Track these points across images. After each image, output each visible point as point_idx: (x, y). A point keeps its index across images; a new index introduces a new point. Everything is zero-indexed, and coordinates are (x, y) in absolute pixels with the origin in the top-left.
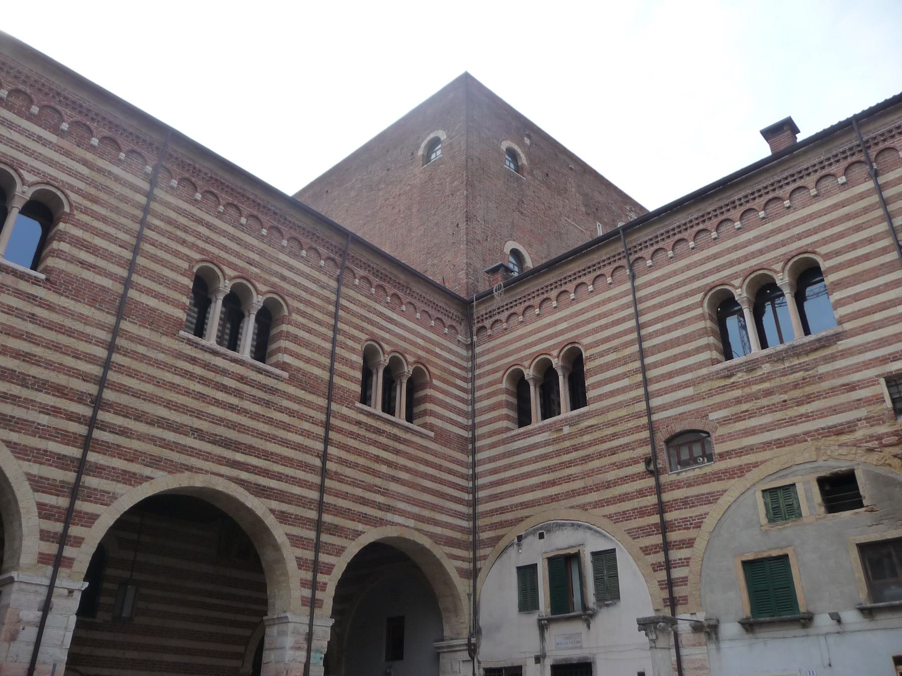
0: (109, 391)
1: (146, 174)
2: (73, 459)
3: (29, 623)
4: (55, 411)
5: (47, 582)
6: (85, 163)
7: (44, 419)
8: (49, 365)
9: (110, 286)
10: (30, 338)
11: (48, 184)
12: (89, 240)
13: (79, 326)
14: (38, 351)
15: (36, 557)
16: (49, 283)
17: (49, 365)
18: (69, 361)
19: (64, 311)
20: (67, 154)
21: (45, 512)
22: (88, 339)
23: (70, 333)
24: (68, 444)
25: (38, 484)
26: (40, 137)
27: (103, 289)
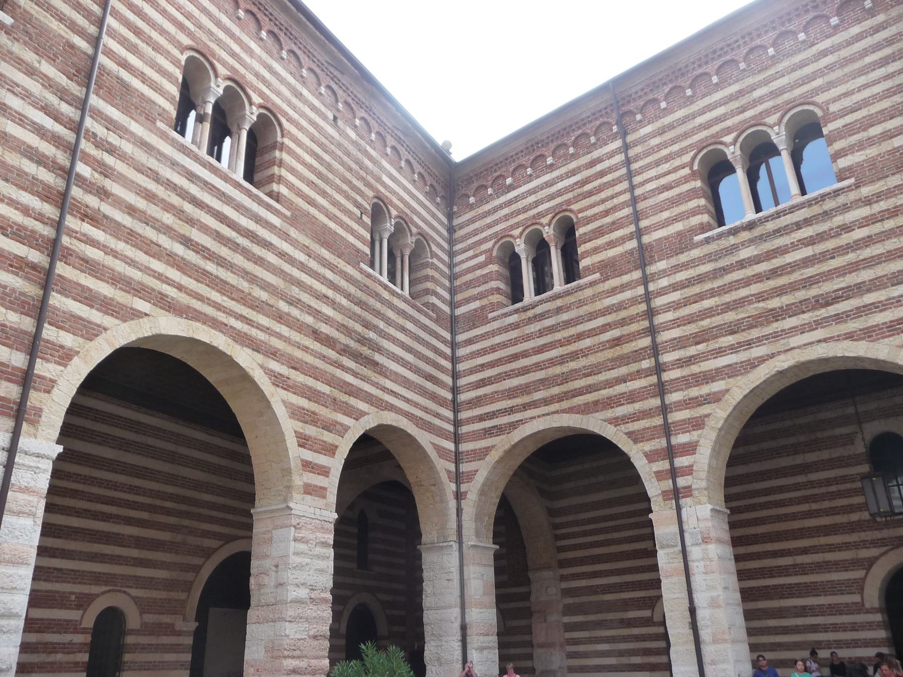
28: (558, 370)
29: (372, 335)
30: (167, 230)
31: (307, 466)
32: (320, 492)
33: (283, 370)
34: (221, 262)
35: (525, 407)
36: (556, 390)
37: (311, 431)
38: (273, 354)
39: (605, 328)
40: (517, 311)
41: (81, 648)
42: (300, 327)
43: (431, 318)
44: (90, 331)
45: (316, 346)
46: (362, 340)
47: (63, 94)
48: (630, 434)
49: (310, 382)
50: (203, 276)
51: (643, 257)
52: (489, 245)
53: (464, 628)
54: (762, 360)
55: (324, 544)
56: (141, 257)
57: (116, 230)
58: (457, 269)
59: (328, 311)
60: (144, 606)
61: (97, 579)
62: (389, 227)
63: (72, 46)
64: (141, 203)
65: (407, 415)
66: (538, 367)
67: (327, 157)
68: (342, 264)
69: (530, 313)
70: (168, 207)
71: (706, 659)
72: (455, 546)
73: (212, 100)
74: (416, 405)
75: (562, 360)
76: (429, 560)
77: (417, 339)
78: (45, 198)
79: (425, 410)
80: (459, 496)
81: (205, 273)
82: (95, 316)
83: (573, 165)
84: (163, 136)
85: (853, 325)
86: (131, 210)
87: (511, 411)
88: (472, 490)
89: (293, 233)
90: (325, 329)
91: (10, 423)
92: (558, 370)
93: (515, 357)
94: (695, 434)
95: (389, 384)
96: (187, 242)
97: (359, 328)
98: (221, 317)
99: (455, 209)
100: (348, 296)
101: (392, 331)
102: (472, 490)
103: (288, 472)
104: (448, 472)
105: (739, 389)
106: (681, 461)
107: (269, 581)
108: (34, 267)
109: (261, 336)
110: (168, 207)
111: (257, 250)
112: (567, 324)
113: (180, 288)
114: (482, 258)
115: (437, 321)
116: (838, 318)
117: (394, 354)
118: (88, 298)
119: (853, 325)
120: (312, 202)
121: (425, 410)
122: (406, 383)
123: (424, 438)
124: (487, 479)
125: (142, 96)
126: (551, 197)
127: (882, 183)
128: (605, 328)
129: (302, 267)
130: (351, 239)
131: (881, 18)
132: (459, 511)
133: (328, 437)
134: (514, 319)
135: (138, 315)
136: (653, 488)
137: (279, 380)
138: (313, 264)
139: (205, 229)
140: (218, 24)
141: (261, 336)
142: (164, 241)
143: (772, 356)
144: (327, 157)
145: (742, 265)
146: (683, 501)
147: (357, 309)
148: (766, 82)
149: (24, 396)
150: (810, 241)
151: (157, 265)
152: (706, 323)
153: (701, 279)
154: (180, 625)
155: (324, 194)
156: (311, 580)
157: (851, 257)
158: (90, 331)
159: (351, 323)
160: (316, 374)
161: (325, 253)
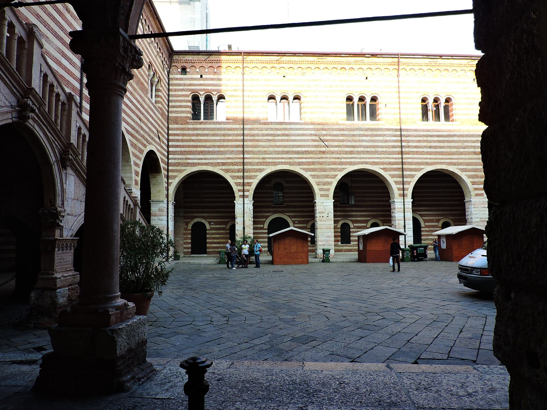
33: (465, 167)
34: (441, 147)
38: (461, 164)
42: (469, 153)
44: (412, 176)
49: (474, 167)
56: (420, 156)
57: (414, 153)
61: (440, 215)
64: (417, 144)
70: (424, 141)
78: (398, 154)
82: (413, 173)
86: (416, 147)
96: (430, 147)
98: (443, 161)
103: (470, 192)
109: (456, 161)
110: (424, 141)
113: (431, 159)
118: (411, 170)
135: (422, 169)
137: (463, 170)
139: (434, 141)
141: (456, 161)
158: (412, 176)
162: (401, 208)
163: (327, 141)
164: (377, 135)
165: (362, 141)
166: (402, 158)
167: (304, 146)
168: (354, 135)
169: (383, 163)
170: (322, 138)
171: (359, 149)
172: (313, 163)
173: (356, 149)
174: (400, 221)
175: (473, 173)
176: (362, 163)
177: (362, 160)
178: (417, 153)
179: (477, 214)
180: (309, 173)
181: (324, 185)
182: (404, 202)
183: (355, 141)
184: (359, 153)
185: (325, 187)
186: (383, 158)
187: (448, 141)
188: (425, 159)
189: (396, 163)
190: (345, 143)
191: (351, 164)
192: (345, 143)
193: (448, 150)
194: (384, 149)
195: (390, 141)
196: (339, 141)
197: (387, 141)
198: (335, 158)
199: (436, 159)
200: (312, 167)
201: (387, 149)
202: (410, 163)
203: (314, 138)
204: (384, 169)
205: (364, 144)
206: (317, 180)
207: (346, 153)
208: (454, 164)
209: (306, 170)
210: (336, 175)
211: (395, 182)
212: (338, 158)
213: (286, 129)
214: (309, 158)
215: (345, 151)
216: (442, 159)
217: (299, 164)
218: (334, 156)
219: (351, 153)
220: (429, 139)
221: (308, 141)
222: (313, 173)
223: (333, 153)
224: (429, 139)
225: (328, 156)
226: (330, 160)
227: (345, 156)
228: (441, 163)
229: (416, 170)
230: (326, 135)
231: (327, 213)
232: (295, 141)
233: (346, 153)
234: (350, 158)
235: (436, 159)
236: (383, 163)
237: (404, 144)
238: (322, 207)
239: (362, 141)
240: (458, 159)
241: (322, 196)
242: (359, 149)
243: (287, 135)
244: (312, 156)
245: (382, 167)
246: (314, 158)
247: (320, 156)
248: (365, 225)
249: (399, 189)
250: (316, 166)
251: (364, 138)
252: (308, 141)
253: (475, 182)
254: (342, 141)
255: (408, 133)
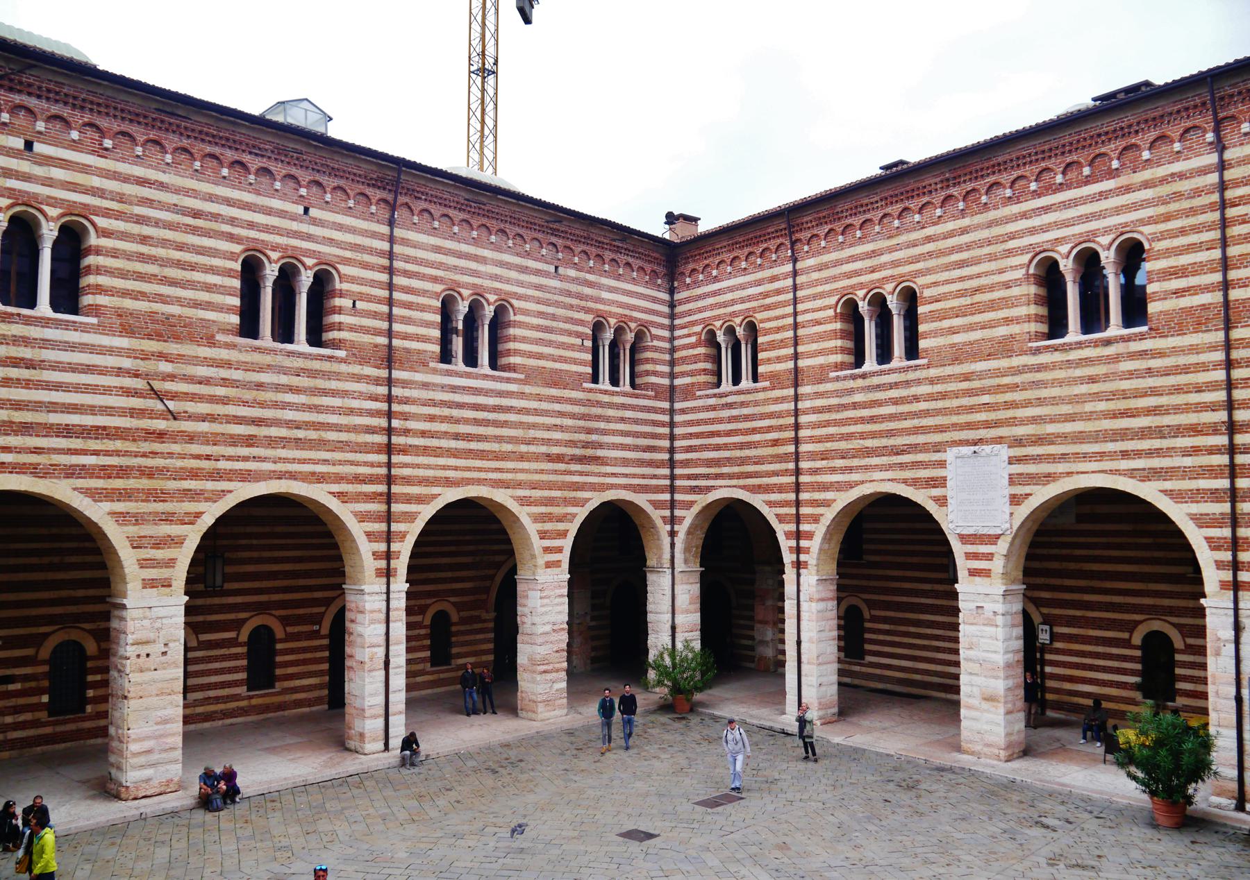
0: (1242, 411)
1: (1210, 144)
2: (1224, 491)
3: (1226, 641)
4: (1196, 451)
5: (1232, 605)
6: (1146, 185)
7: (1188, 461)
8: (1177, 409)
9: (1210, 301)
10: (1154, 392)
11: (1122, 234)
12: (1175, 264)
13: (1193, 359)
14: (1163, 400)
15: (1218, 584)
16: (1156, 332)
17: (1177, 409)
18: (1194, 398)
19: (1175, 351)
20: (1128, 189)
21: (1214, 544)
22: (1204, 367)
23: (1186, 369)
24: (1216, 478)
25: (1201, 521)
26: (1101, 193)
27: (1204, 307)
28: (738, 453)
29: (594, 437)
30: (445, 435)
31: (547, 550)
32: (557, 564)
33: (527, 493)
35: (718, 476)
36: (736, 469)
37: (549, 526)
38: (519, 485)
39: (769, 429)
40: (715, 396)
41: (425, 637)
42: (536, 457)
43: (649, 398)
44: (410, 517)
45: (550, 466)
46: (586, 445)
47: (377, 381)
48: (777, 515)
49: (546, 493)
50: (470, 454)
51: (797, 378)
52: (698, 329)
53: (673, 628)
54: (857, 484)
55: (562, 596)
58: (676, 343)
59: (557, 435)
60: (459, 607)
62: (608, 335)
63: (376, 346)
65: (625, 487)
66: (725, 447)
67: (550, 310)
68: (567, 393)
69: (724, 400)
70: (444, 419)
71: (803, 673)
72: (669, 571)
73: (461, 317)
74: (634, 476)
75: (742, 446)
76: (651, 578)
77: (636, 421)
78: (379, 452)
79: (643, 477)
80: (673, 534)
81: (471, 451)
82: (412, 508)
83: (760, 275)
84: (435, 371)
85: (908, 474)
86: (423, 434)
87: (707, 477)
88: (682, 529)
89: (527, 389)
90: (555, 450)
91: (384, 580)
92: (738, 453)
93: (713, 434)
94: (814, 525)
95: (609, 469)
96: (457, 437)
97: (583, 437)
98: (483, 475)
99: (676, 284)
100: (573, 416)
101: (612, 426)
102: (682, 529)
103: (533, 557)
104: (663, 518)
105: (843, 499)
106: (803, 543)
107: (528, 620)
108: (381, 494)
111: (502, 417)
112: (747, 418)
113: (456, 468)
114: (693, 339)
115: (656, 398)
116: (902, 466)
117: (615, 444)
118: (409, 499)
119: (908, 474)
120: (540, 356)
121: (643, 477)
122: (625, 462)
123: (641, 500)
124: (692, 524)
125: (419, 352)
126: (742, 300)
127: (941, 369)
128: (769, 429)
129: (537, 412)
130: (574, 368)
131: (966, 222)
132: (673, 545)
133: (561, 526)
134: (712, 401)
135: (435, 496)
136: (788, 558)
137: (524, 501)
138: (544, 406)
139: (467, 421)
140: (460, 255)
142: (444, 443)
143: (863, 482)
144: (550, 310)
145: (855, 406)
146: (802, 571)
147: (581, 423)
148: (891, 250)
149: (389, 564)
150: (896, 402)
151: (441, 461)
152: (829, 445)
153: (829, 409)
154: (485, 616)
155: (549, 343)
156: (553, 619)
157: (916, 422)
158: (410, 517)
159: (577, 437)
160: (550, 486)
161: (554, 392)
162: (380, 611)
163: (174, 396)
164: (325, 392)
165: (285, 406)
166: (389, 465)
167: (92, 410)
168: (260, 386)
169: (339, 479)
170: (157, 385)
171: (274, 432)
172: (123, 472)
173: (263, 431)
174: (375, 650)
175: (543, 509)
176: (280, 476)
177: (280, 467)
178: (425, 451)
179: (546, 613)
180: (107, 506)
181: (157, 546)
182: (388, 593)
183: (262, 405)
184: (272, 442)
185: (159, 554)
186: (341, 463)
187: (496, 424)
188: (444, 468)
189: (371, 480)
190: (231, 410)
191: (245, 476)
192: (231, 410)
193: (495, 447)
194: (344, 436)
195: (360, 412)
196: (213, 399)
197: (351, 412)
198: (198, 457)
199: (469, 469)
200: (118, 483)
201: (351, 437)
202: (408, 481)
203: (128, 382)
204: (340, 495)
205: (289, 415)
206: (132, 530)
207: (234, 440)
208: (505, 484)
209: (95, 495)
210: (198, 515)
211: (368, 534)
212: (208, 457)
213: (26, 341)
214: (107, 453)
215: (232, 436)
216: (480, 470)
217: (71, 472)
218: (195, 449)
219: (250, 441)
220: (456, 413)
221: (107, 390)
222: (120, 507)
223: (191, 438)
224: (456, 413)
225: (176, 448)
226: (179, 463)
227: (231, 451)
228: (479, 482)
229: (420, 500)
230: (171, 377)
231: (162, 641)
232: (57, 387)
233: (234, 440)
234: (246, 459)
235: (469, 469)
236: (339, 479)
237: (395, 423)
238: (146, 623)
239: (285, 406)
240: (514, 471)
241: (150, 584)
242: (274, 432)
243: (30, 364)
244: (119, 445)
245: (336, 488)
246: (127, 453)
247: (146, 447)
248: (232, 635)
249: (376, 555)
250: (131, 483)
251: (289, 398)
252: (107, 390)
253: (546, 532)
254: (224, 401)
255: (407, 393)
